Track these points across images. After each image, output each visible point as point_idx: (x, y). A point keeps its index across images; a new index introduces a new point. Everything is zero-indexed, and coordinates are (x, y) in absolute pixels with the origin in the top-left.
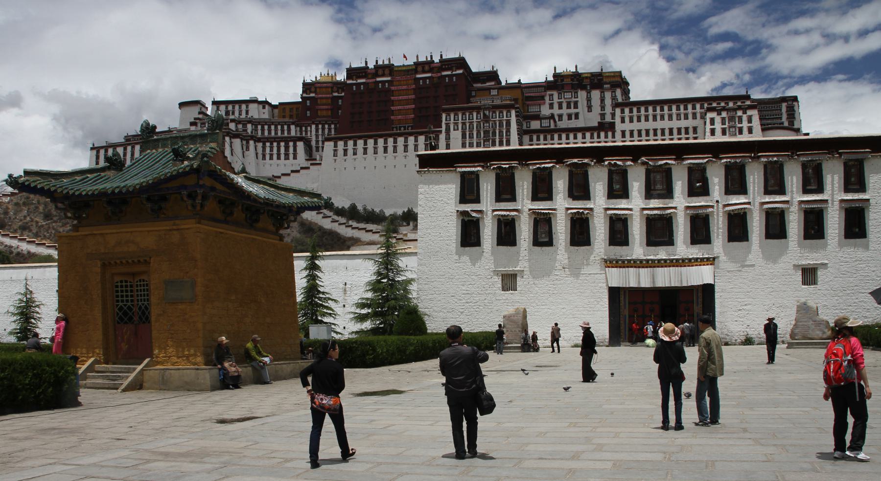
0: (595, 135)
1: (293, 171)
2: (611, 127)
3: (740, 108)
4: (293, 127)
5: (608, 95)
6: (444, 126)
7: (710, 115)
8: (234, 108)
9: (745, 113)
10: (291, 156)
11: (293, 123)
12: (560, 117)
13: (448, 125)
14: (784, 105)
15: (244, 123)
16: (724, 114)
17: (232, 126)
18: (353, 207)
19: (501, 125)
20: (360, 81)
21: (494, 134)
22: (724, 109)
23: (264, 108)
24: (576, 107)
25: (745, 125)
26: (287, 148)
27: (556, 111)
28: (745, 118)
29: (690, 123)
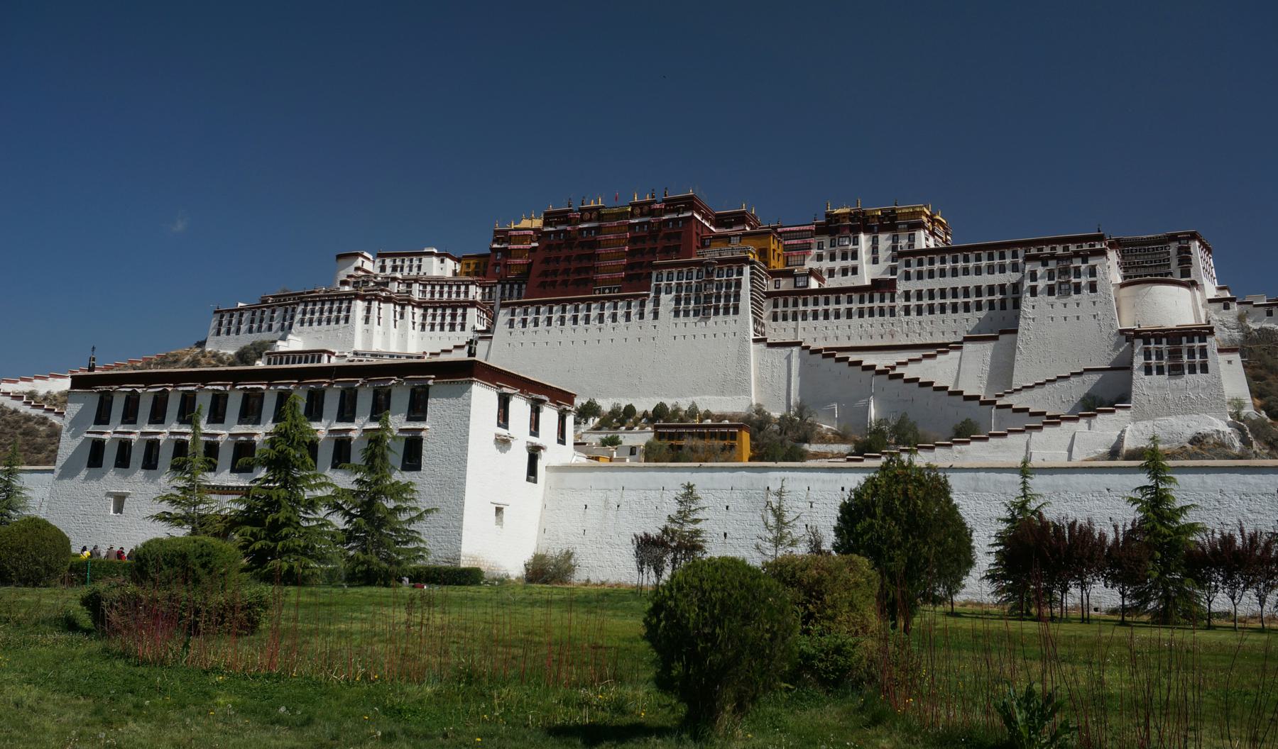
0: (867, 296)
1: (456, 347)
3: (1076, 254)
4: (472, 288)
7: (1028, 267)
8: (403, 261)
9: (1085, 261)
10: (458, 328)
11: (473, 283)
12: (831, 273)
14: (1173, 247)
15: (408, 282)
16: (1052, 264)
20: (560, 228)
21: (718, 299)
22: (1053, 257)
23: (442, 261)
24: (855, 255)
26: (454, 316)
29: (1009, 278)
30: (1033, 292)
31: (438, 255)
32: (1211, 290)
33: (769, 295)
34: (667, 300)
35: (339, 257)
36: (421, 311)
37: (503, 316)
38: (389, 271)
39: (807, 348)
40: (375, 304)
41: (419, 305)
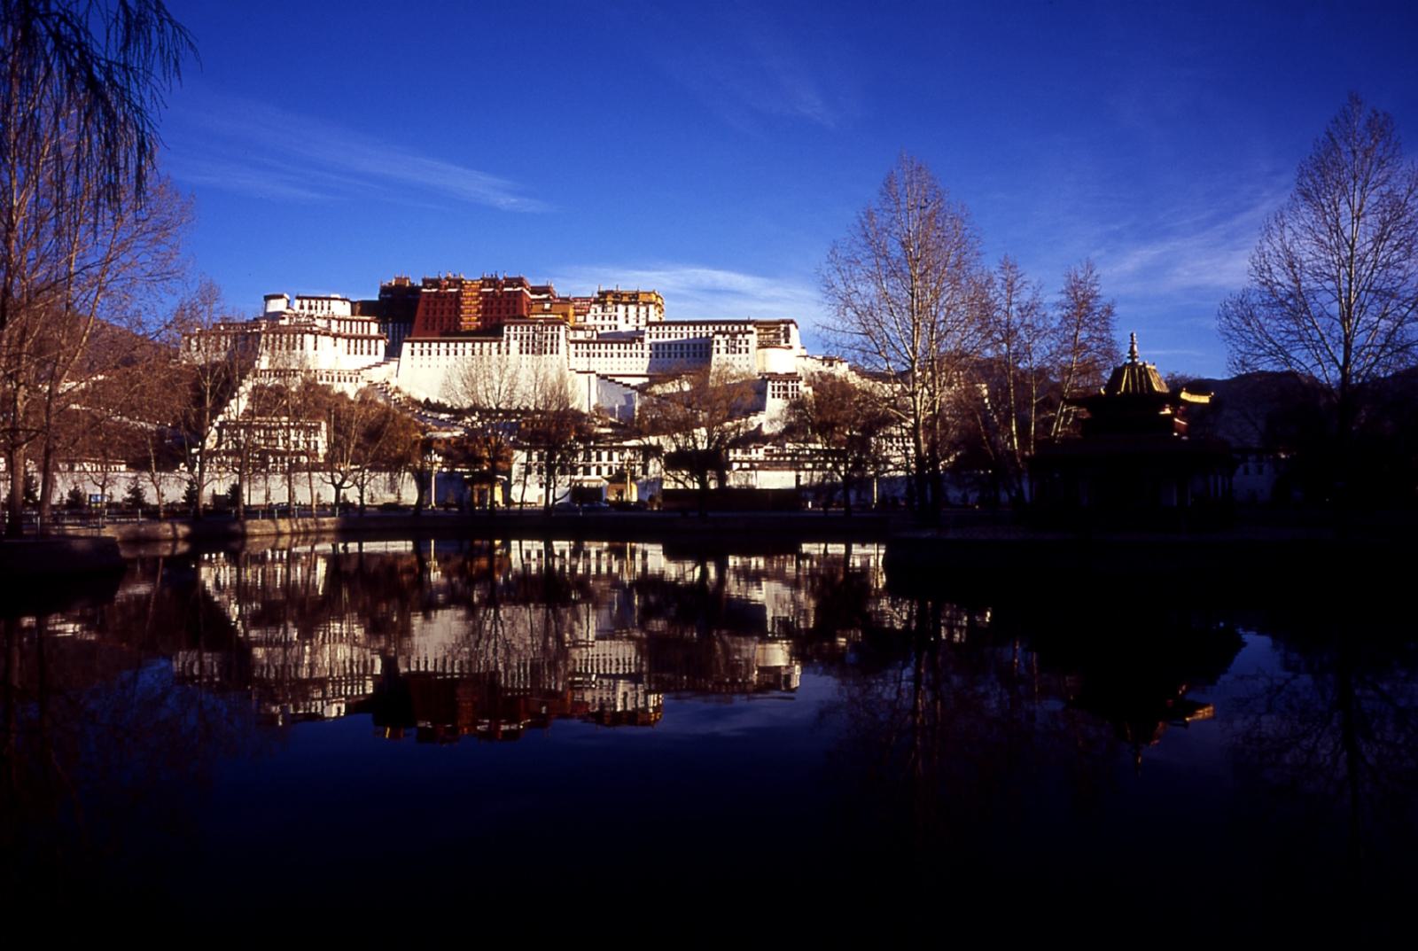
2: (642, 340)
3: (740, 332)
5: (643, 309)
6: (505, 337)
7: (718, 337)
13: (508, 338)
14: (783, 326)
16: (727, 337)
17: (318, 322)
18: (427, 400)
19: (552, 338)
22: (728, 333)
24: (616, 319)
25: (743, 345)
27: (599, 321)
28: (744, 342)
30: (718, 352)
31: (342, 300)
32: (797, 350)
33: (572, 342)
34: (515, 345)
35: (268, 298)
36: (346, 341)
37: (406, 347)
38: (306, 311)
39: (598, 375)
40: (319, 337)
41: (345, 337)
